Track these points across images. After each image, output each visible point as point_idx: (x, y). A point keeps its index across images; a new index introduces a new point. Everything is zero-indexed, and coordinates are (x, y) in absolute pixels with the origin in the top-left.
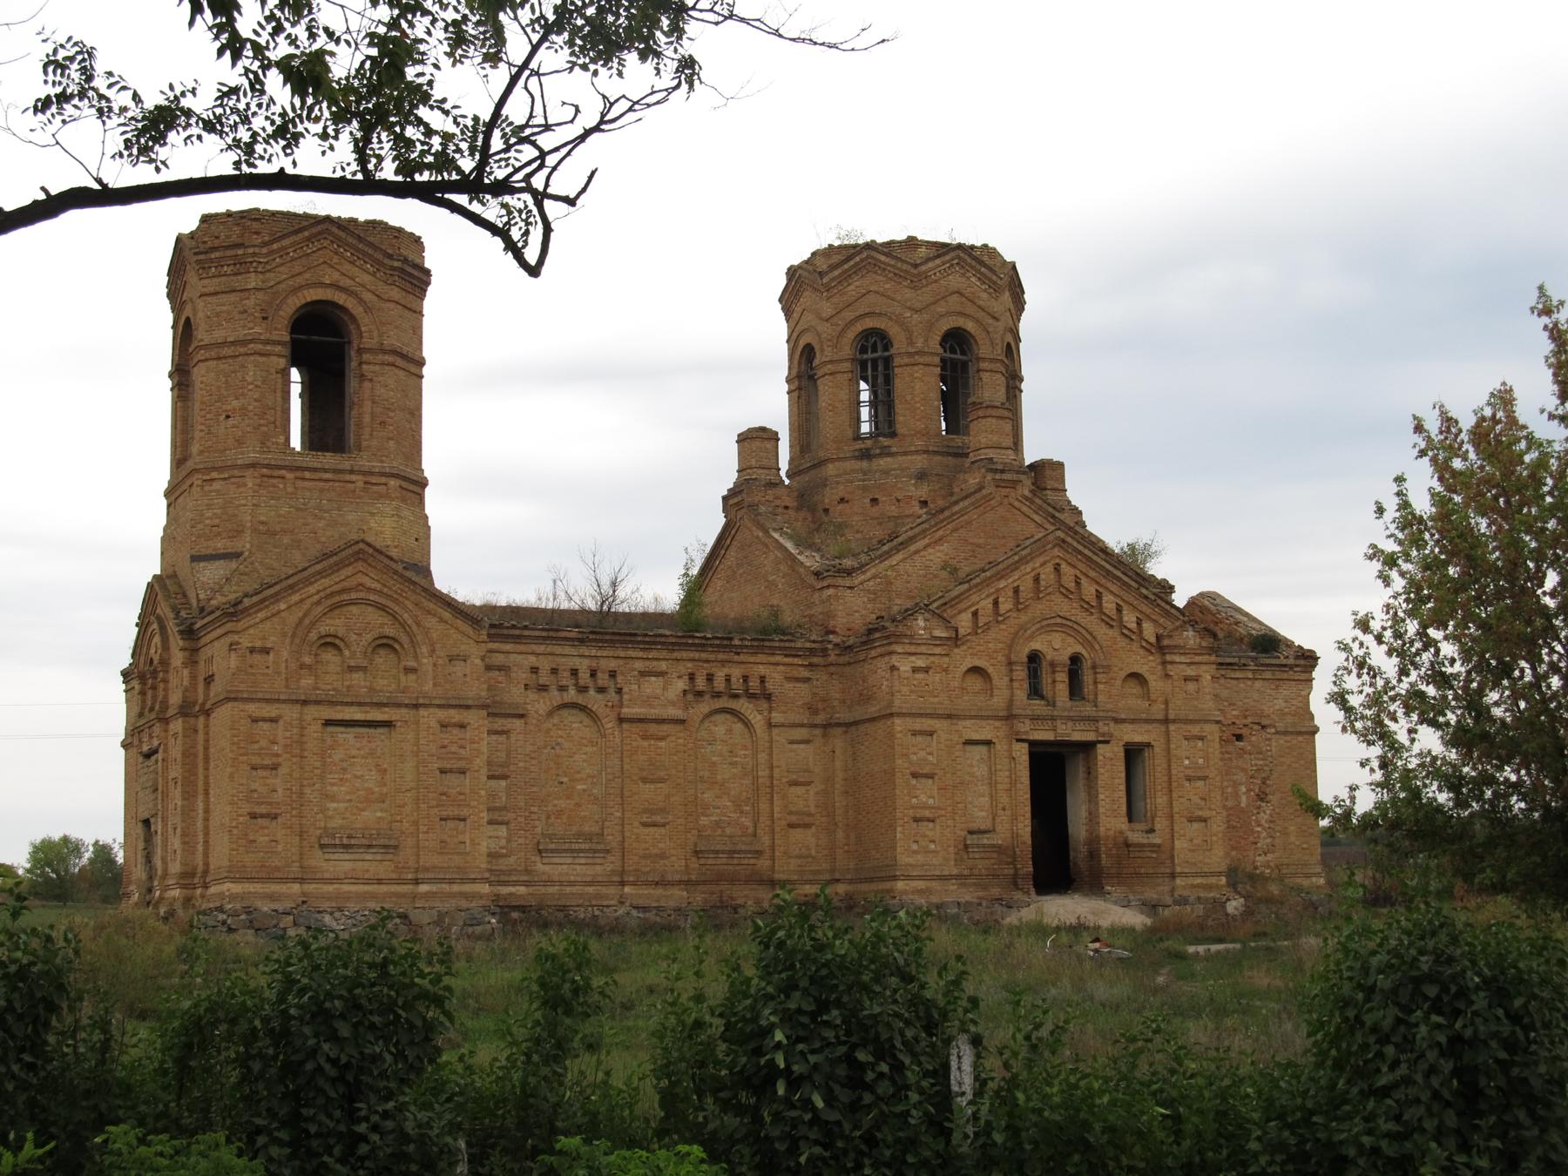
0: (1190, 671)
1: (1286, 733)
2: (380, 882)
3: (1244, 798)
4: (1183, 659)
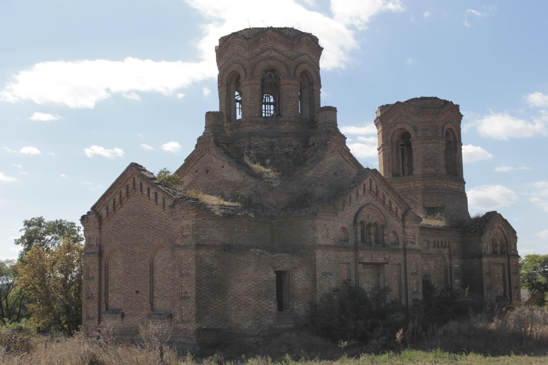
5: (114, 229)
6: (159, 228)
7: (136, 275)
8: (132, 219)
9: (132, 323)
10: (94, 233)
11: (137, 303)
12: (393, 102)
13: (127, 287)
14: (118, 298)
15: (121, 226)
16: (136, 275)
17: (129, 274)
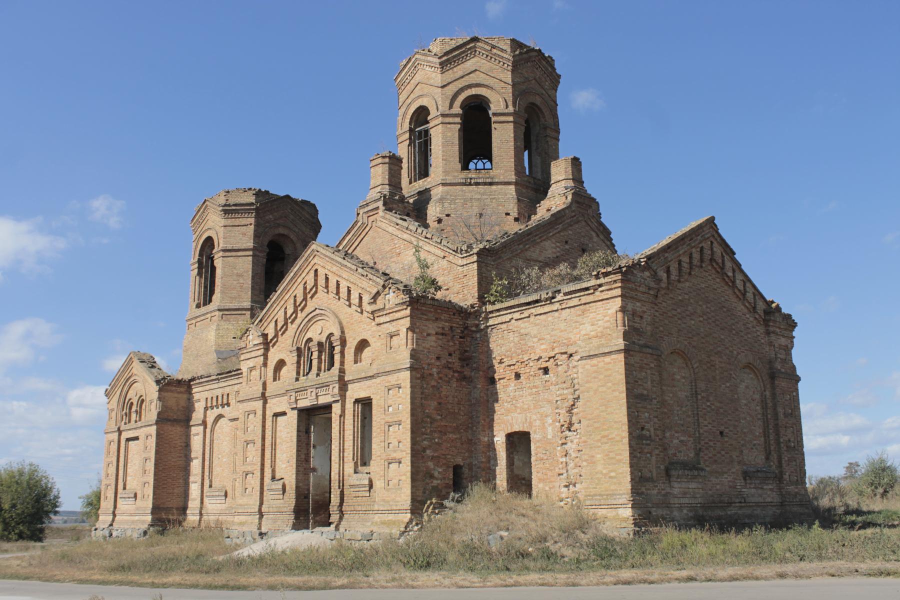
0: (391, 328)
1: (590, 357)
2: (131, 515)
3: (550, 429)
4: (387, 318)
5: (674, 312)
6: (746, 337)
7: (718, 405)
8: (704, 306)
9: (718, 487)
10: (645, 309)
11: (723, 453)
12: (282, 194)
13: (706, 422)
14: (681, 441)
15: (688, 313)
16: (718, 405)
17: (708, 401)
